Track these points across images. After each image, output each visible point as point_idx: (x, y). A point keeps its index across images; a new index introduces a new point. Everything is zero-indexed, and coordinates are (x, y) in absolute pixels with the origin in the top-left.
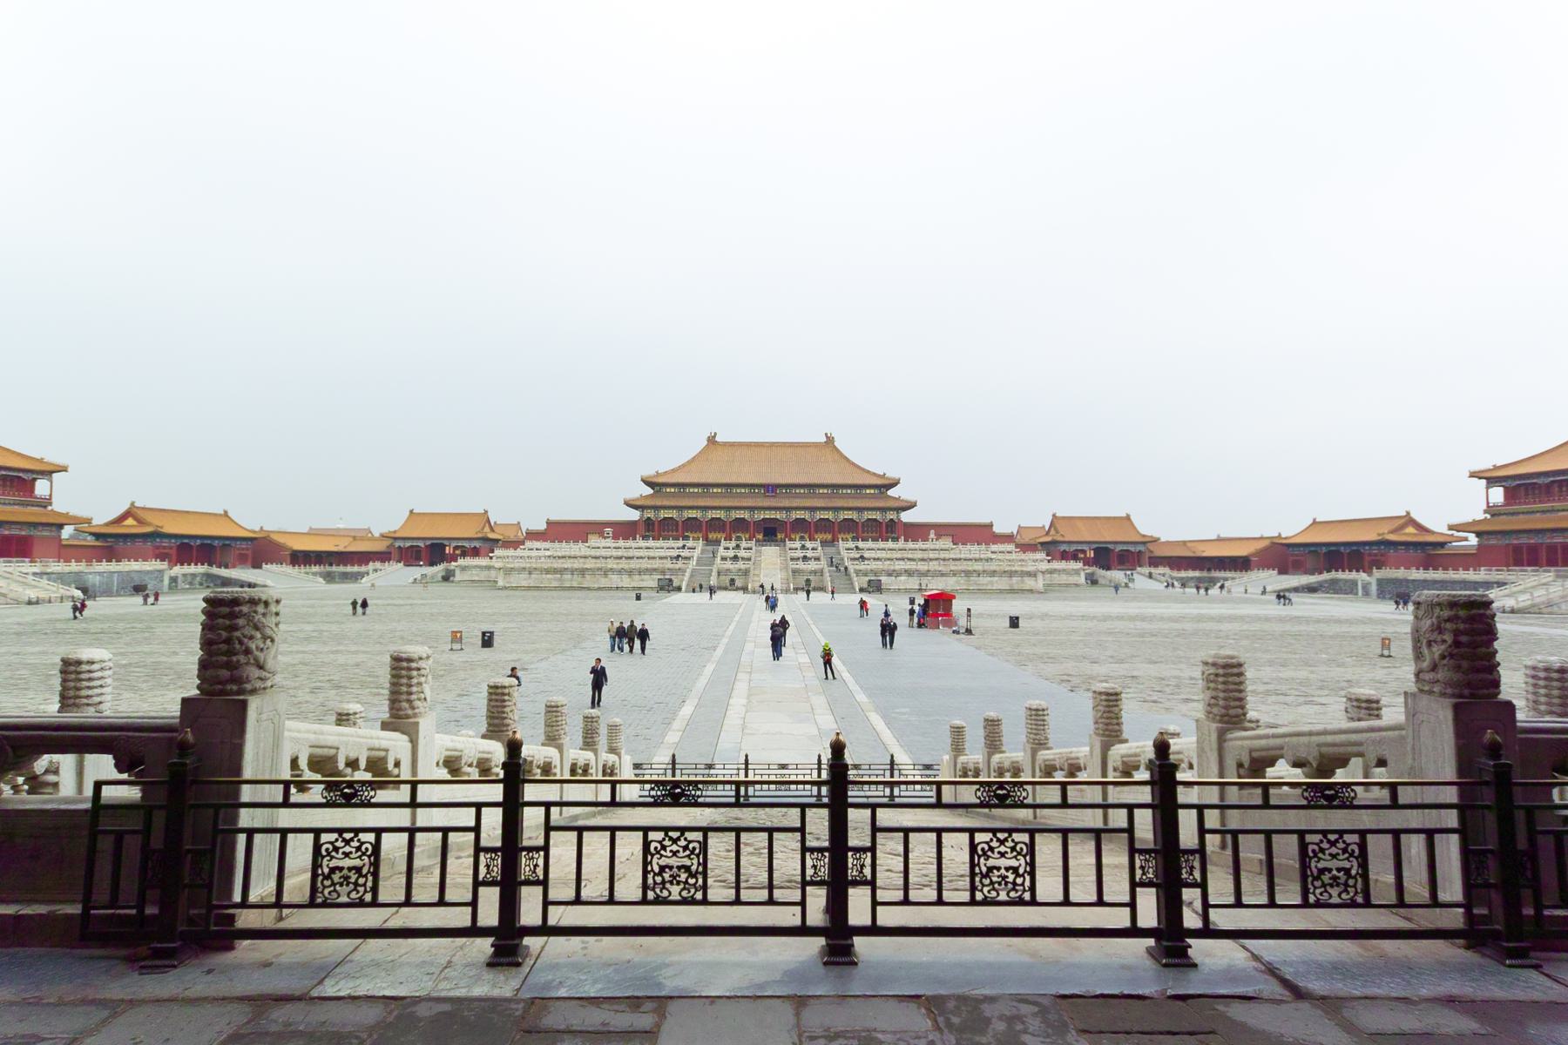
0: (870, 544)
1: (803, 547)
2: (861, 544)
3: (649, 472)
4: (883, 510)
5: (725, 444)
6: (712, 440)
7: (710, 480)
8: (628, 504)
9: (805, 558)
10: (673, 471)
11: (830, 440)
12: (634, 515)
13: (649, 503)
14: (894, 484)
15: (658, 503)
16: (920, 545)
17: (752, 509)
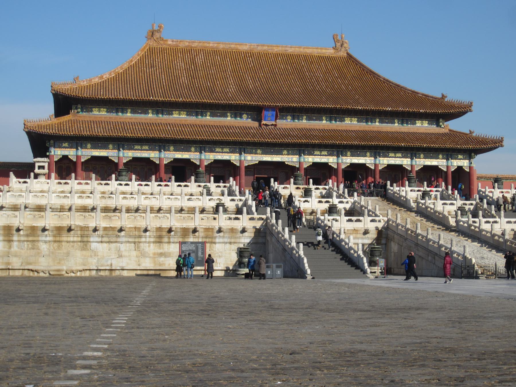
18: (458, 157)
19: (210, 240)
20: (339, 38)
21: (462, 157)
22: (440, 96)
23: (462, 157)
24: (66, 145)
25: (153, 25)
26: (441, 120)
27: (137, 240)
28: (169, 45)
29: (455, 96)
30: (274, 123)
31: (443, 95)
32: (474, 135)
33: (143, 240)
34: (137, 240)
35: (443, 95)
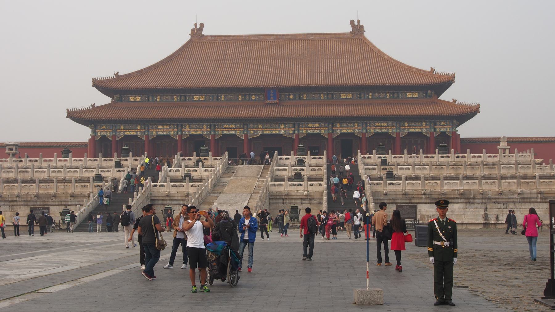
0: (405, 158)
1: (301, 162)
2: (390, 158)
3: (107, 73)
4: (432, 119)
5: (215, 39)
6: (197, 32)
7: (189, 83)
8: (75, 116)
9: (298, 177)
10: (141, 73)
11: (358, 29)
12: (82, 134)
13: (103, 115)
14: (446, 83)
15: (115, 115)
16: (485, 157)
17: (245, 122)
18: (440, 123)
19: (64, 203)
20: (356, 23)
21: (445, 124)
22: (430, 70)
23: (445, 124)
24: (104, 127)
25: (196, 25)
26: (429, 92)
27: (11, 204)
28: (209, 40)
29: (442, 69)
30: (277, 101)
31: (432, 68)
32: (457, 103)
33: (15, 203)
34: (11, 204)
35: (432, 68)
